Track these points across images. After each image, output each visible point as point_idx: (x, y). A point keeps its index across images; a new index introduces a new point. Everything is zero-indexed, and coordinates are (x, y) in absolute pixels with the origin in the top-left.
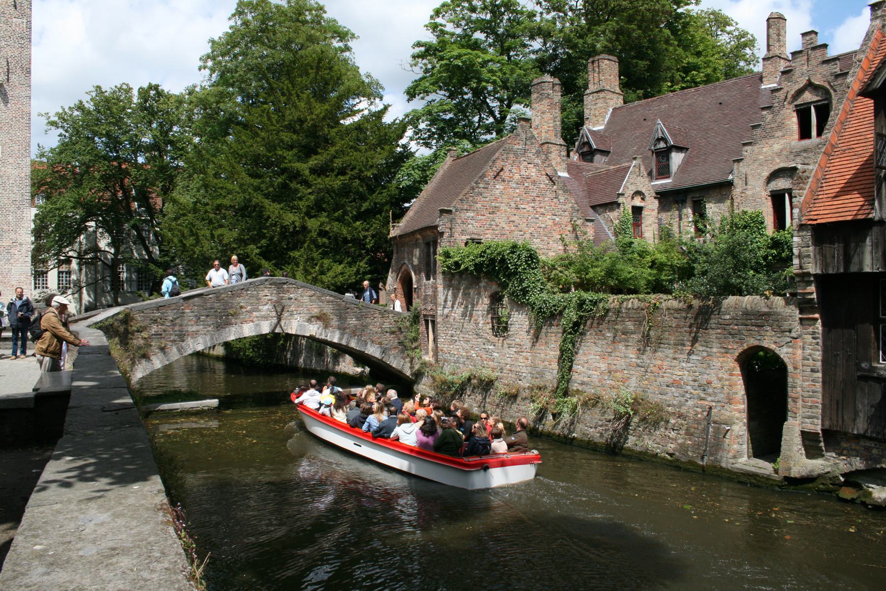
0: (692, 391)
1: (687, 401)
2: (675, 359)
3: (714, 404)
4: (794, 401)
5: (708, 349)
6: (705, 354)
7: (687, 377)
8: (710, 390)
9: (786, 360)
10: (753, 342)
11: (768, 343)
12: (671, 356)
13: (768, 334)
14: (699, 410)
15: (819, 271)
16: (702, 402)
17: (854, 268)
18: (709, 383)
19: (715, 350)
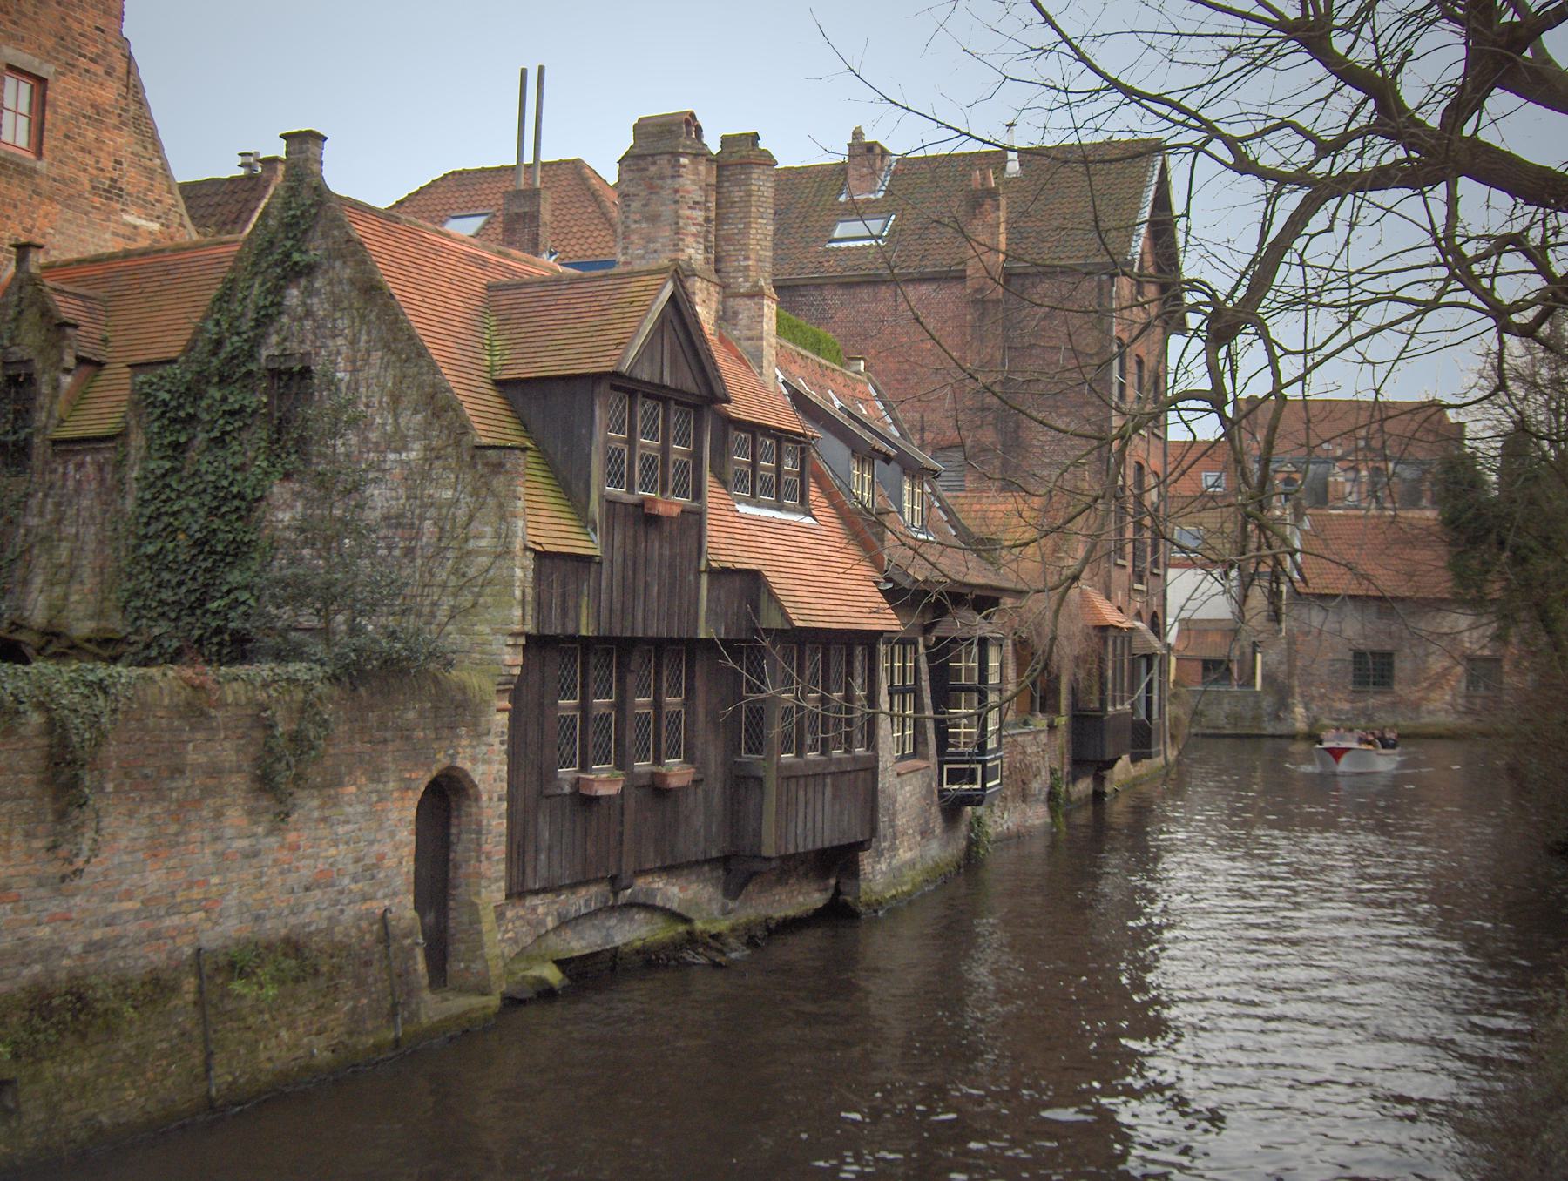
0: (353, 886)
1: (342, 911)
2: (324, 819)
3: (387, 902)
4: (488, 858)
5: (380, 786)
6: (374, 798)
7: (341, 854)
8: (382, 875)
9: (481, 787)
10: (442, 761)
11: (464, 763)
12: (316, 814)
13: (464, 742)
14: (364, 924)
15: (534, 632)
16: (368, 904)
17: (570, 630)
18: (381, 857)
19: (391, 785)
